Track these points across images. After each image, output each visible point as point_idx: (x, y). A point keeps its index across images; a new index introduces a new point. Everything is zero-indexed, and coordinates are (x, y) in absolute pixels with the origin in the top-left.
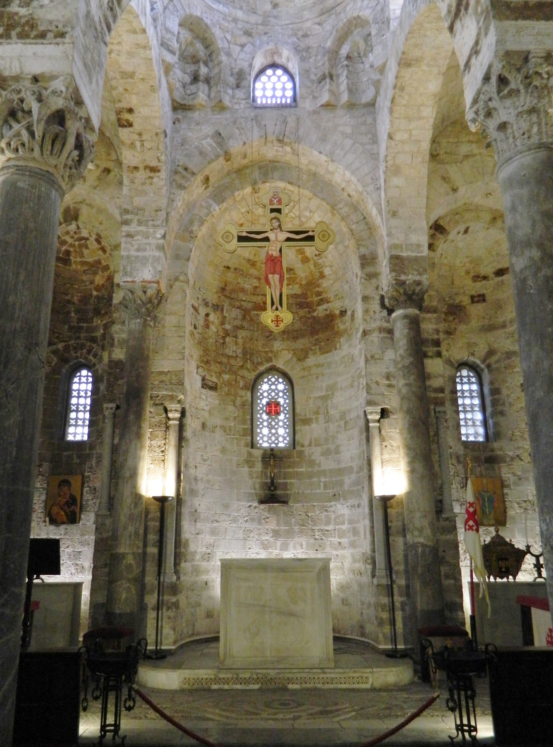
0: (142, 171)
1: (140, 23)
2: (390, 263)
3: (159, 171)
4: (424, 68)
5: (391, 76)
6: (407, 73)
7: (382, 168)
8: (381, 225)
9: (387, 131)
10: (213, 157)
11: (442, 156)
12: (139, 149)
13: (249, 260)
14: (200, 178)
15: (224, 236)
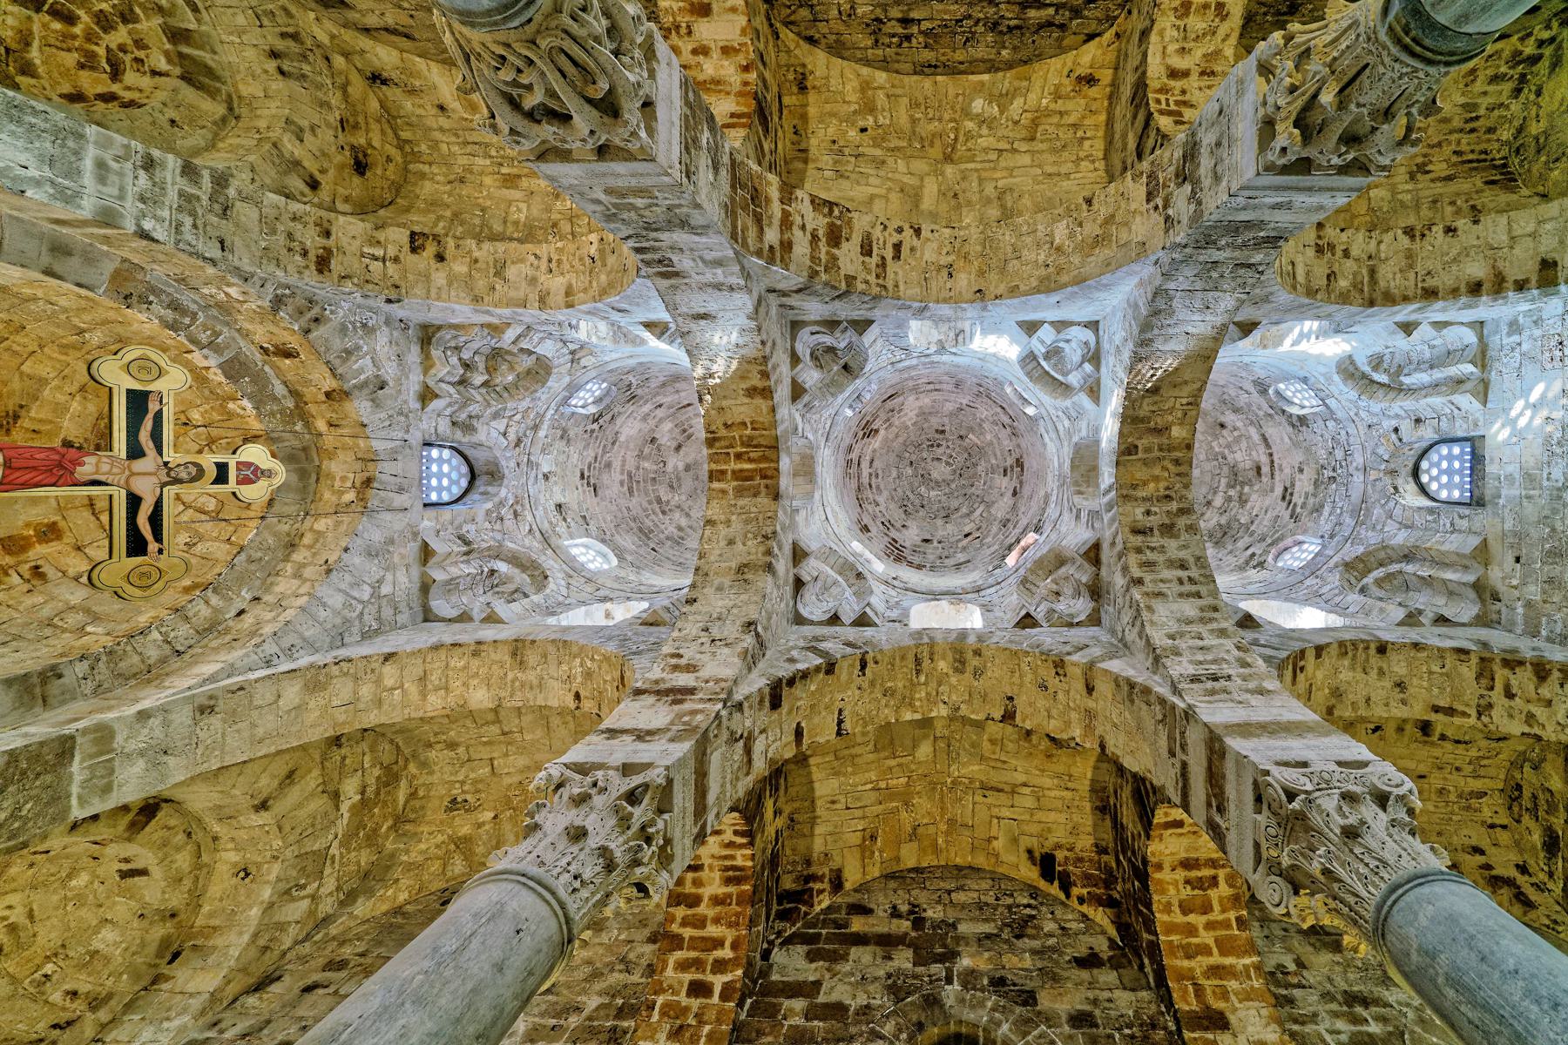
0: (322, 241)
1: (584, 303)
2: (42, 744)
3: (320, 271)
4: (510, 676)
5: (489, 633)
6: (503, 655)
7: (319, 659)
8: (171, 691)
9: (399, 649)
10: (339, 371)
11: (336, 755)
12: (366, 250)
13: (16, 417)
14: (294, 342)
15: (148, 364)
